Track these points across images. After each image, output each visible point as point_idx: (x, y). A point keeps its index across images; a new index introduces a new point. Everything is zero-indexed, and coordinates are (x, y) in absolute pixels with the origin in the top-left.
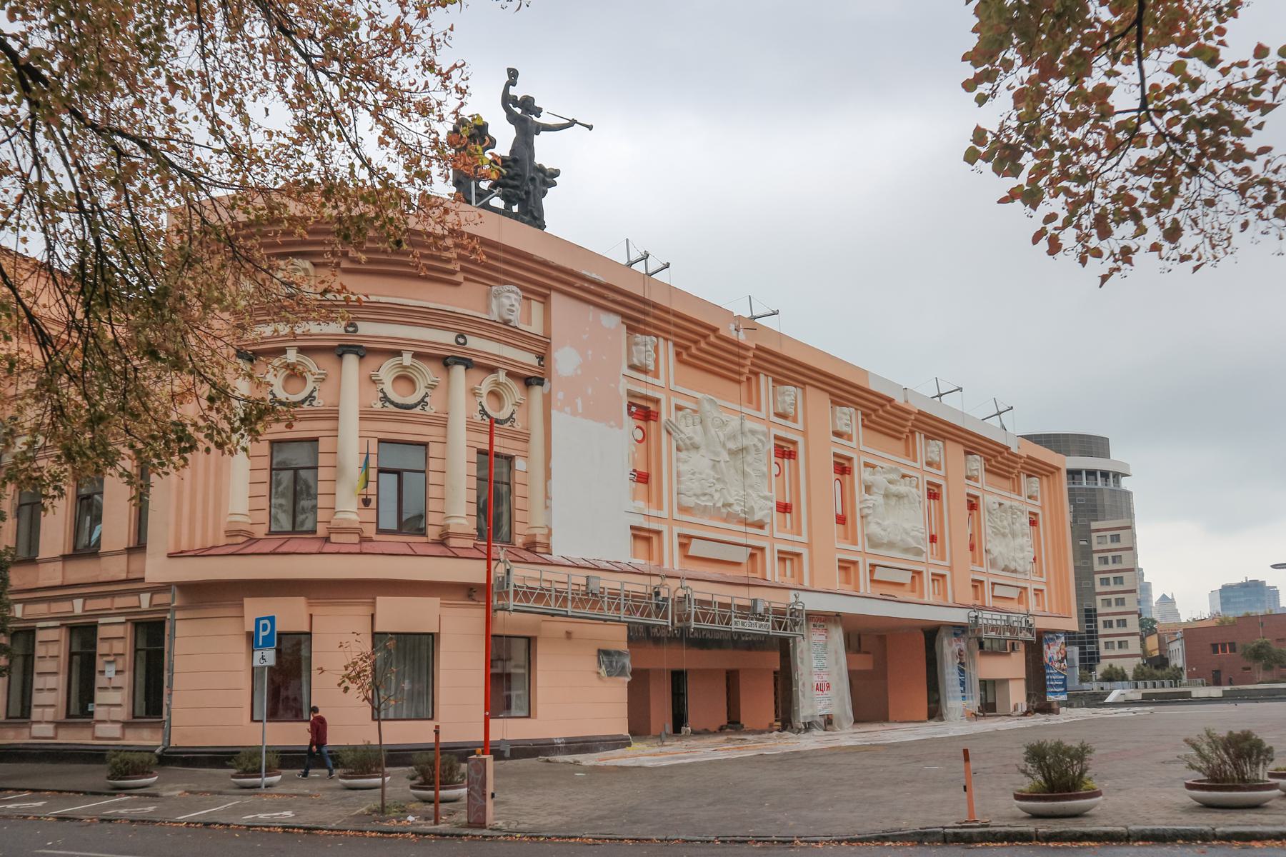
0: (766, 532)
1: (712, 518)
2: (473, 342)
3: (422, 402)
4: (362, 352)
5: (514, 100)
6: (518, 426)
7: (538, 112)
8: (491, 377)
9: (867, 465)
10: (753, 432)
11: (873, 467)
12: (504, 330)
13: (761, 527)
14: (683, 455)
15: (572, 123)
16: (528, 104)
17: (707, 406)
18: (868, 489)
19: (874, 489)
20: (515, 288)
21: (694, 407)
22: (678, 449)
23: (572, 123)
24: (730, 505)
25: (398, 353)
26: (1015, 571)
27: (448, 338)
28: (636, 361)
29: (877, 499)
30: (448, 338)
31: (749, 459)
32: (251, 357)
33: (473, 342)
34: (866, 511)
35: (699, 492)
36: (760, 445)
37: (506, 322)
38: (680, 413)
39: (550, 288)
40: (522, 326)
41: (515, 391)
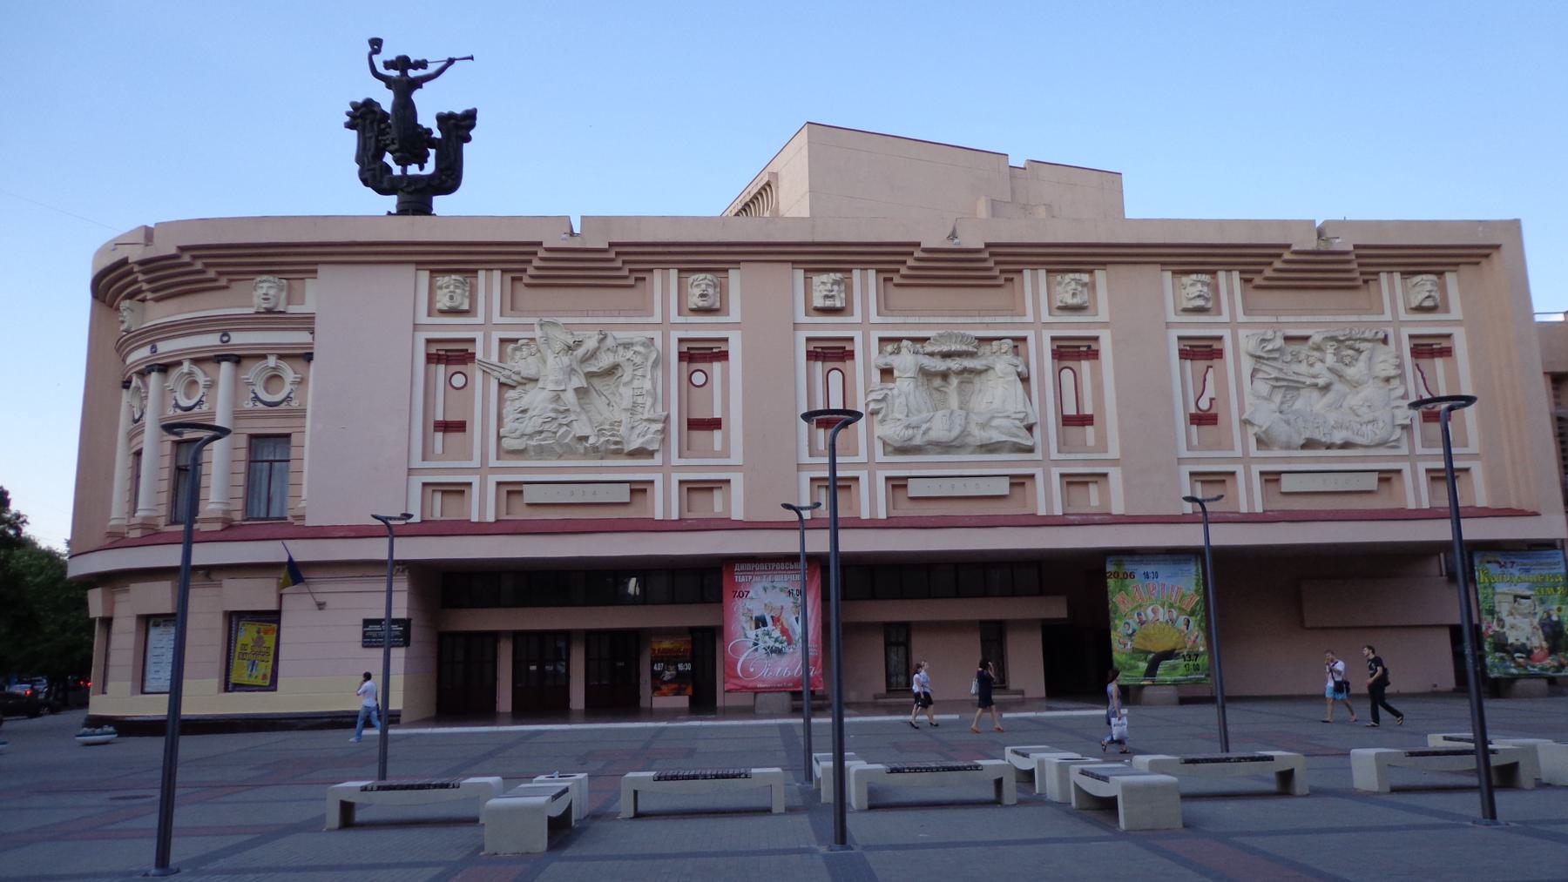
0: (658, 460)
1: (560, 457)
2: (238, 338)
3: (200, 402)
4: (164, 369)
5: (388, 65)
6: (294, 404)
7: (423, 64)
8: (260, 365)
9: (882, 340)
10: (627, 346)
11: (899, 340)
12: (270, 317)
13: (651, 454)
14: (511, 394)
15: (451, 61)
16: (403, 63)
17: (538, 333)
18: (887, 373)
19: (896, 373)
20: (265, 277)
21: (529, 335)
22: (501, 385)
23: (451, 61)
24: (586, 438)
25: (179, 363)
26: (1346, 445)
27: (212, 340)
28: (439, 306)
29: (904, 385)
30: (212, 340)
31: (626, 378)
32: (126, 385)
33: (238, 338)
34: (872, 406)
35: (529, 430)
36: (638, 360)
37: (269, 311)
38: (512, 346)
39: (316, 263)
40: (293, 309)
41: (289, 373)
